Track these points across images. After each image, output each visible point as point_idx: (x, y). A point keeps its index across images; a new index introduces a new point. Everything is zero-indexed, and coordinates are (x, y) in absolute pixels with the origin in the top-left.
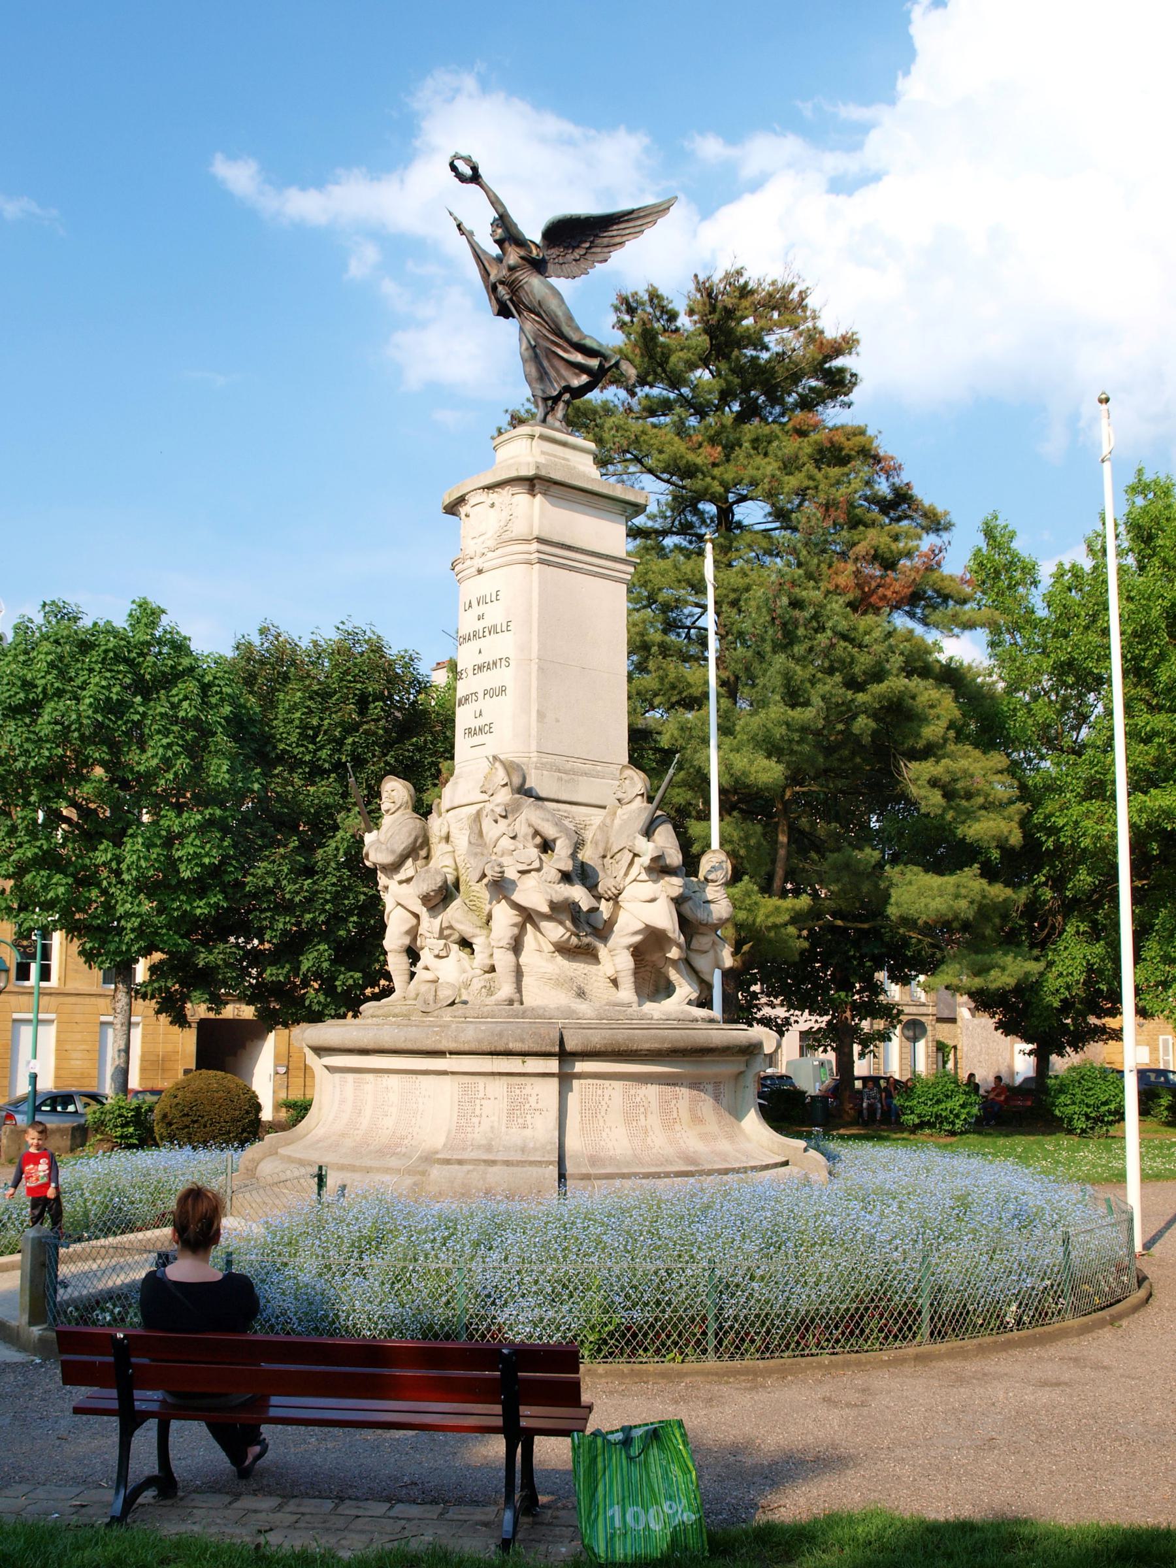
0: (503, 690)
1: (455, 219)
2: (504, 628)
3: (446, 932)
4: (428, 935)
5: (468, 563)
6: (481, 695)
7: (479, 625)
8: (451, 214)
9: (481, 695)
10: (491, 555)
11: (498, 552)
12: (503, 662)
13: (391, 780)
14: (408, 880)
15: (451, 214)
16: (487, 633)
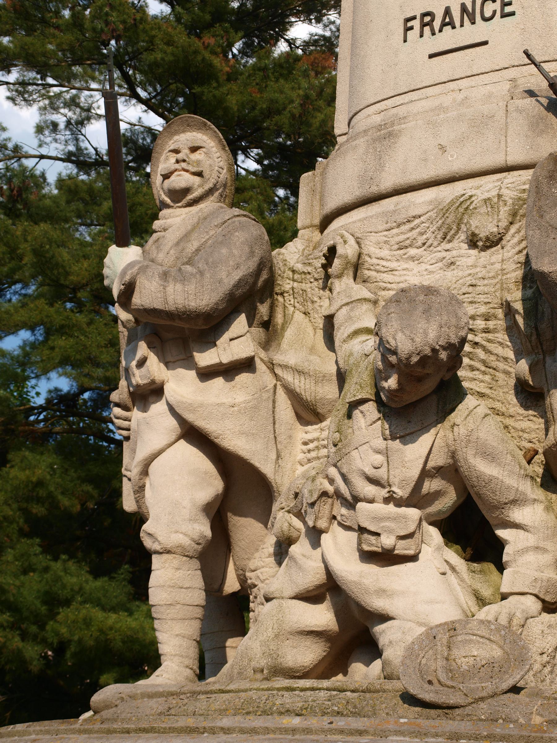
3: (430, 486)
4: (370, 490)
13: (190, 126)
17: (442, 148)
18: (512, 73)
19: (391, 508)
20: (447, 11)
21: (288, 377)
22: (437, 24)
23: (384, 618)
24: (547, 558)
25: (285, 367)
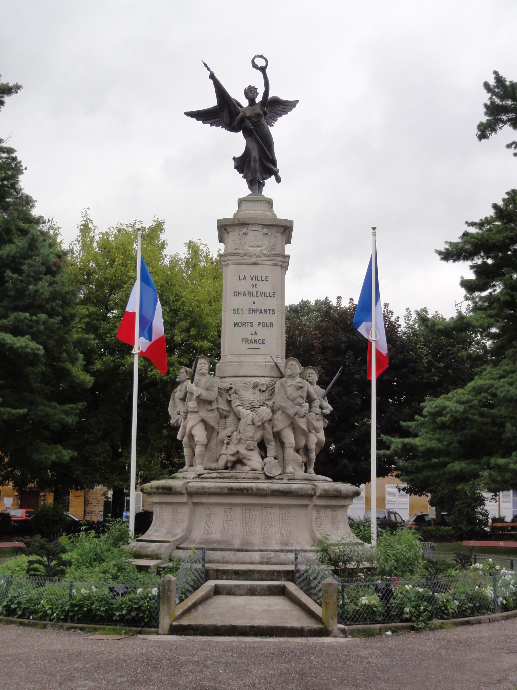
0: (271, 324)
1: (209, 69)
2: (271, 295)
4: (250, 439)
5: (246, 257)
6: (255, 324)
7: (254, 290)
8: (206, 65)
9: (255, 324)
10: (263, 258)
11: (270, 258)
12: (271, 312)
14: (212, 410)
15: (206, 65)
16: (259, 294)
17: (253, 370)
18: (264, 356)
19: (253, 442)
20: (251, 340)
21: (221, 411)
22: (249, 342)
23: (250, 460)
24: (275, 450)
25: (221, 409)
